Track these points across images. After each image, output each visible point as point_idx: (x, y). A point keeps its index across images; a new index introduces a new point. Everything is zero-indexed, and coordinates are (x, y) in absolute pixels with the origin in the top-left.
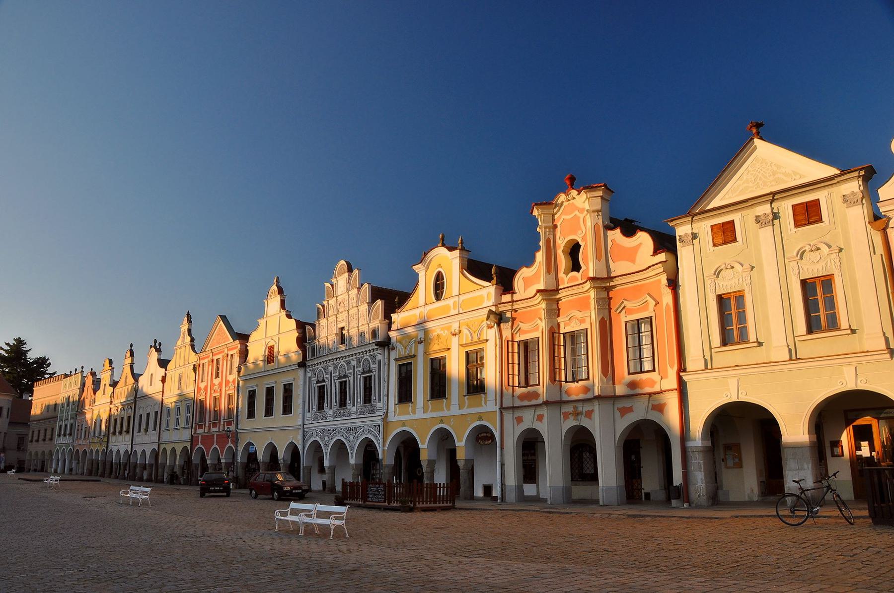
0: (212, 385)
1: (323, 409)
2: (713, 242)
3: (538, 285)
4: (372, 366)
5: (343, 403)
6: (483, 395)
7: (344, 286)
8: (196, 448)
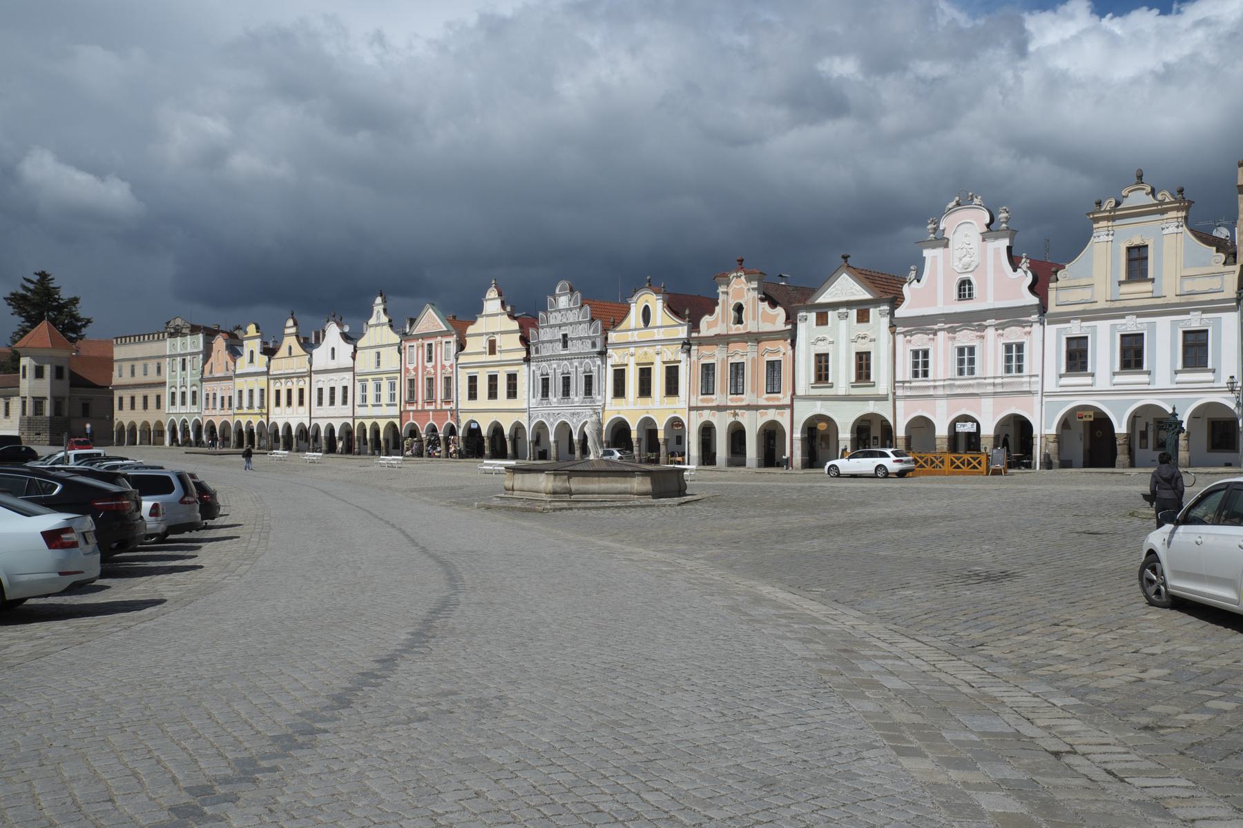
0: (424, 368)
1: (547, 396)
3: (715, 328)
4: (592, 368)
5: (566, 393)
8: (407, 423)
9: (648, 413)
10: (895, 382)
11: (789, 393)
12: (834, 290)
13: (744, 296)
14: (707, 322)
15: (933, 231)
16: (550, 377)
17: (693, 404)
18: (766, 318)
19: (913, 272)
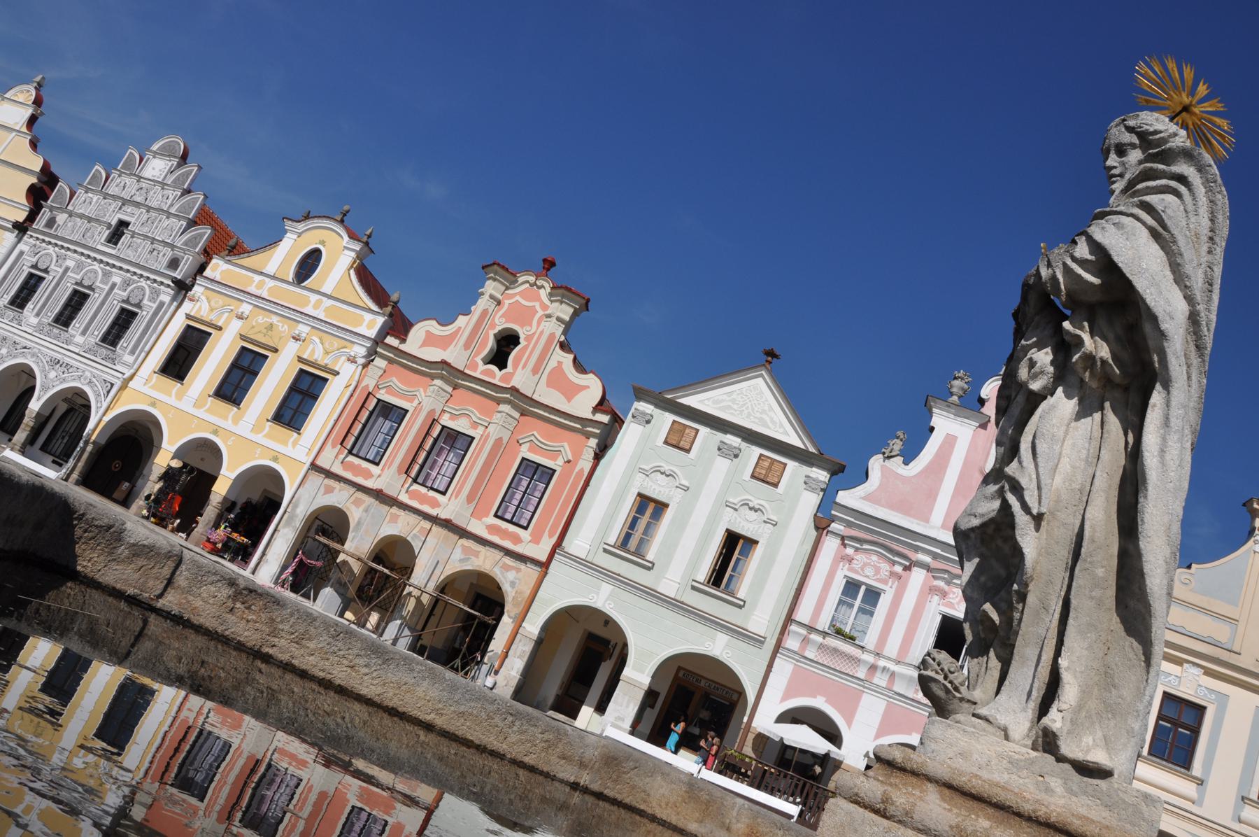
2: (666, 438)
5: (65, 318)
6: (295, 435)
7: (160, 170)
9: (215, 432)
10: (789, 619)
11: (547, 544)
12: (725, 397)
13: (531, 326)
14: (428, 332)
15: (961, 393)
16: (49, 278)
17: (323, 462)
18: (557, 382)
19: (898, 441)
